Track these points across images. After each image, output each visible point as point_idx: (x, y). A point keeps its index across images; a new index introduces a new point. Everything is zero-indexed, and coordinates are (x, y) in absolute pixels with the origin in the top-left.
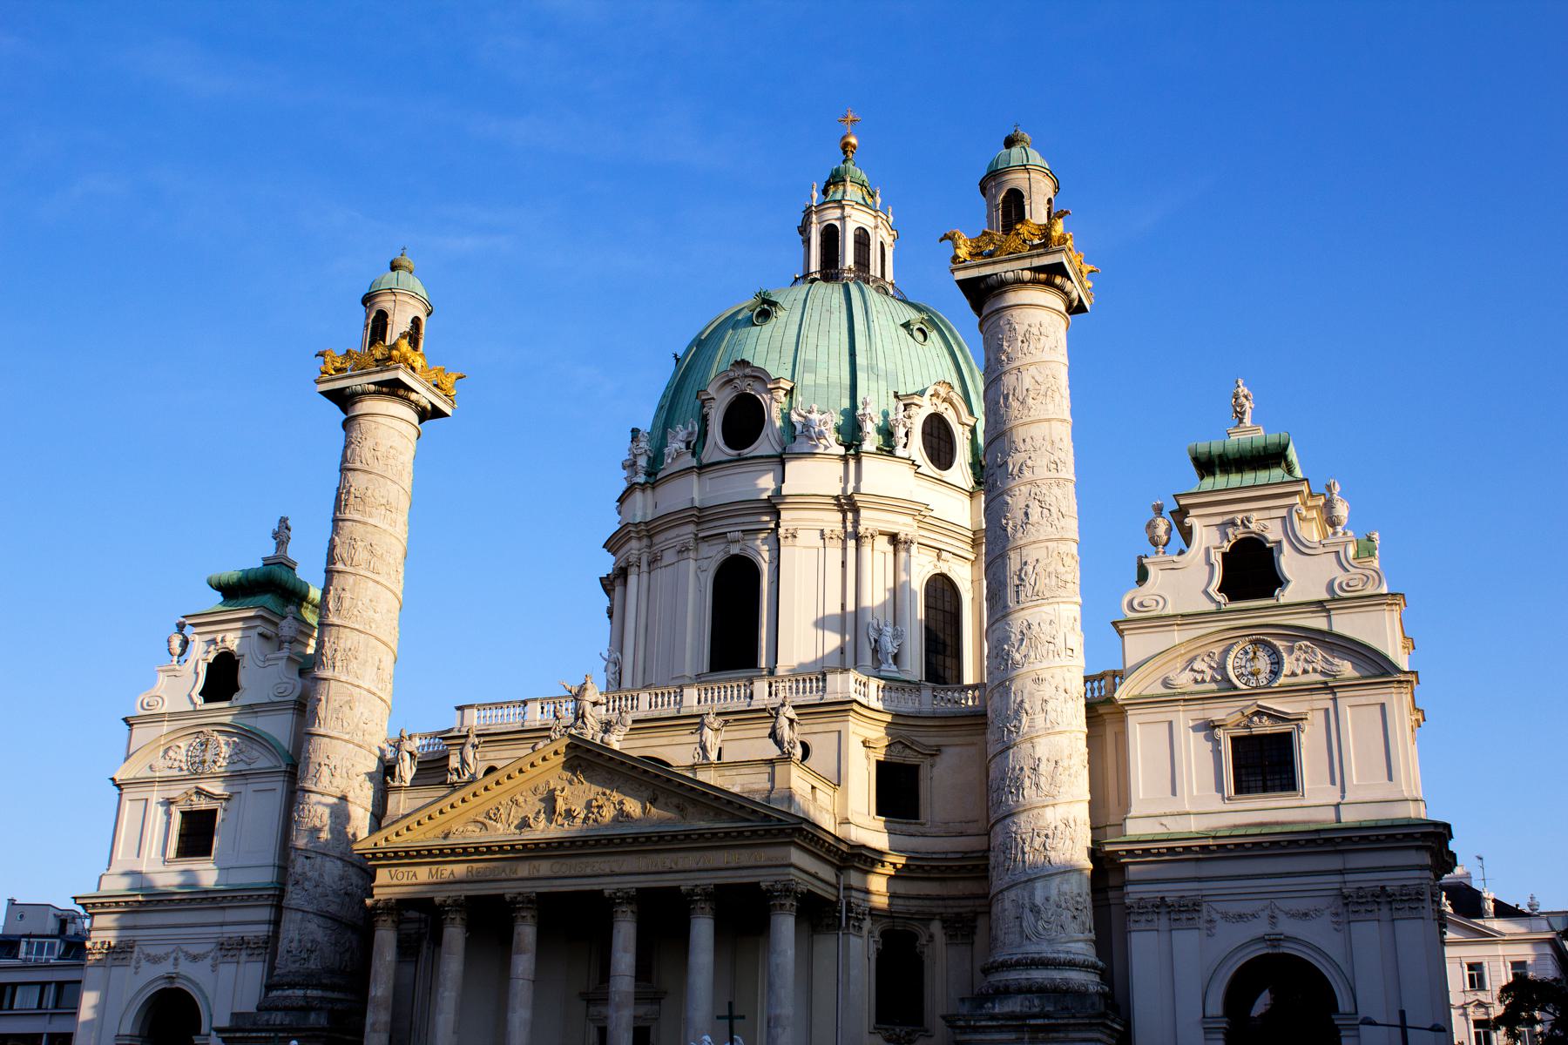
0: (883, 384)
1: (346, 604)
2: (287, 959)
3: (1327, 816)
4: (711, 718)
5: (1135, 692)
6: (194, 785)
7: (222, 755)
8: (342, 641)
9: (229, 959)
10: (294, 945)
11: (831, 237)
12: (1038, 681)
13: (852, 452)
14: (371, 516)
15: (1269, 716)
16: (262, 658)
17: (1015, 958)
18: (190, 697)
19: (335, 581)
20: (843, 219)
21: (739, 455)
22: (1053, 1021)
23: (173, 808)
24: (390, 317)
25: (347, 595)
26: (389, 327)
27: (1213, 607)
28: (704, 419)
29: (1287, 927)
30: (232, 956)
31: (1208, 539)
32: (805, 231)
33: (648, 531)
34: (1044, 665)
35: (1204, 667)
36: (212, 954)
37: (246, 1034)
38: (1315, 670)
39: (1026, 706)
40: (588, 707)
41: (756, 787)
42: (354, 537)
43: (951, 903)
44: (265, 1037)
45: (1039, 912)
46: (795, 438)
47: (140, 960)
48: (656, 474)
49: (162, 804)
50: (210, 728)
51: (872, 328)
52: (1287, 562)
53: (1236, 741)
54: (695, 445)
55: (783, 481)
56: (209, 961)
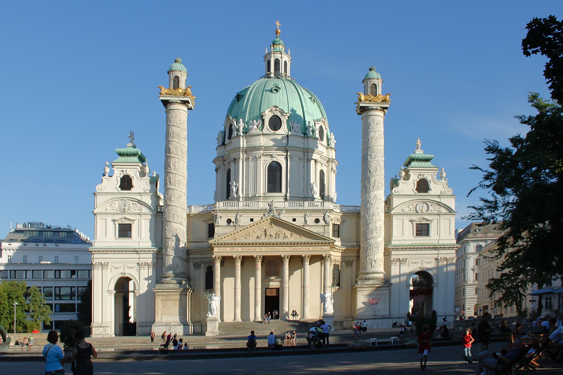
5: (395, 212)
6: (123, 216)
12: (377, 208)
13: (306, 135)
15: (425, 219)
21: (275, 133)
23: (116, 222)
28: (263, 121)
31: (414, 177)
34: (379, 205)
35: (412, 208)
38: (436, 210)
39: (375, 214)
40: (274, 209)
41: (320, 231)
43: (347, 258)
48: (246, 133)
50: (126, 199)
51: (305, 98)
53: (417, 224)
54: (260, 128)
55: (288, 142)
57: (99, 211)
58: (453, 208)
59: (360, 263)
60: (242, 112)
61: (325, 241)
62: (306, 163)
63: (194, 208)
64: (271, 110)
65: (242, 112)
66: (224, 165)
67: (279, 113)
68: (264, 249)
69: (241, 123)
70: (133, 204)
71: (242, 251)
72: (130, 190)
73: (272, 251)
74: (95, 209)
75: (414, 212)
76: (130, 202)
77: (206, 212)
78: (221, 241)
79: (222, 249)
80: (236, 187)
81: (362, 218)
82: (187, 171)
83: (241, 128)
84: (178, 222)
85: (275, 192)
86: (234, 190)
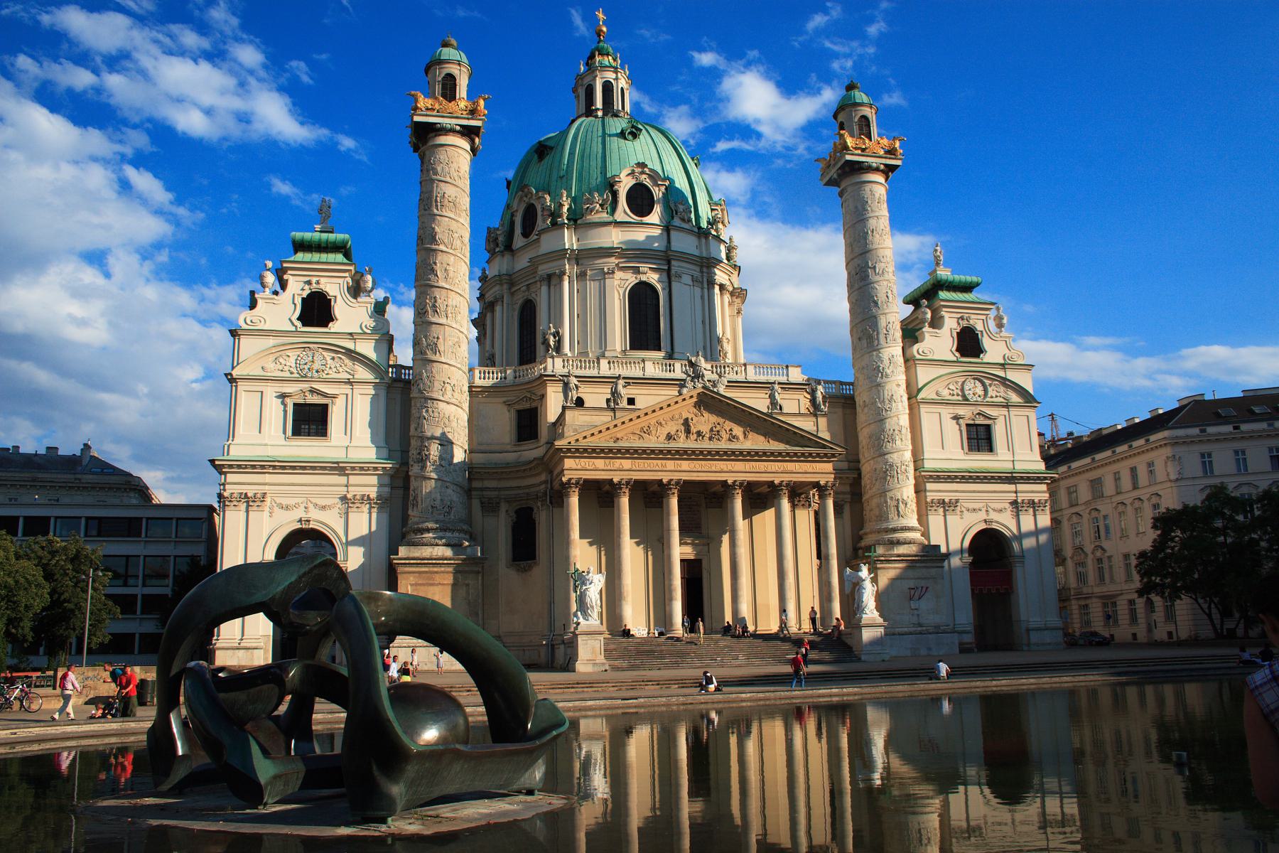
1: (451, 274)
2: (432, 513)
3: (1008, 466)
4: (776, 387)
7: (328, 366)
8: (450, 300)
9: (356, 510)
10: (438, 503)
11: (608, 88)
14: (460, 216)
15: (983, 415)
16: (354, 301)
18: (290, 319)
19: (439, 258)
20: (617, 79)
24: (458, 81)
25: (450, 268)
26: (458, 88)
27: (955, 359)
28: (615, 195)
29: (993, 516)
32: (582, 79)
37: (419, 561)
39: (894, 397)
42: (452, 228)
45: (906, 504)
46: (673, 218)
48: (575, 221)
49: (277, 397)
50: (316, 346)
52: (986, 342)
57: (245, 373)
58: (1031, 392)
61: (825, 451)
62: (706, 290)
63: (480, 373)
64: (632, 173)
65: (561, 178)
66: (512, 294)
67: (648, 180)
68: (685, 465)
69: (564, 199)
70: (333, 359)
71: (634, 468)
73: (703, 469)
74: (233, 368)
75: (960, 398)
76: (325, 354)
78: (583, 443)
79: (584, 463)
80: (555, 337)
84: (453, 401)
85: (647, 348)
86: (552, 343)
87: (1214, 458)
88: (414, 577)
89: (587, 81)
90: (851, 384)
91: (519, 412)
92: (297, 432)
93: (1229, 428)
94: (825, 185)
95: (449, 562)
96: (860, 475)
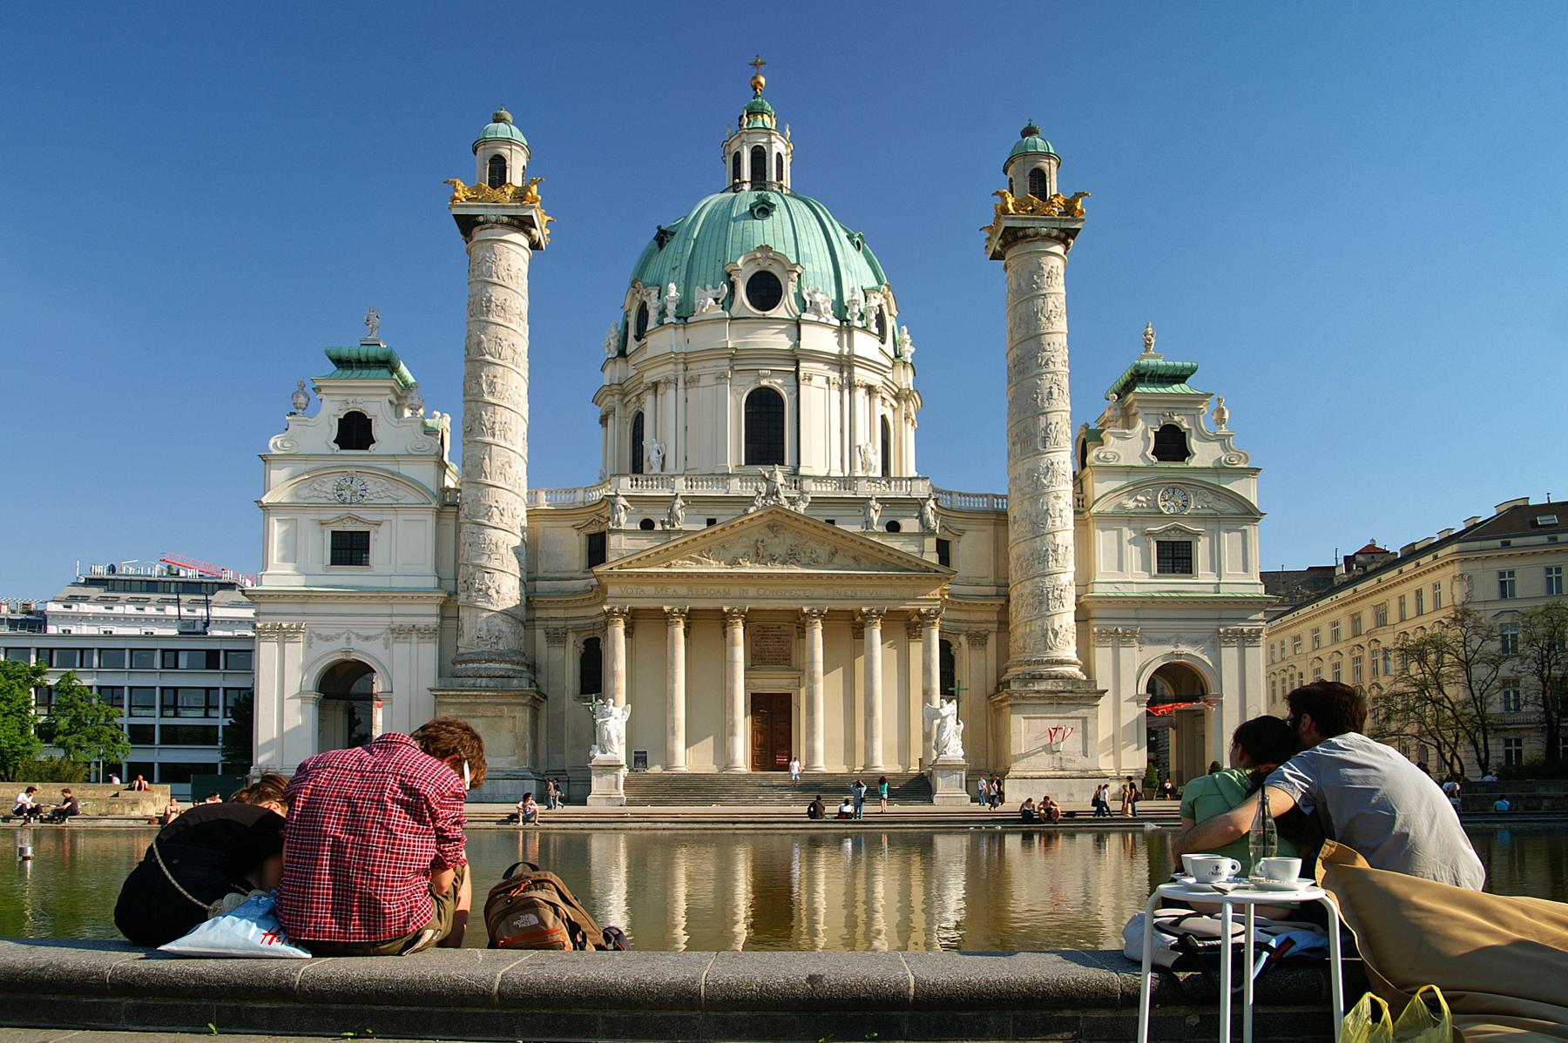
0: (854, 277)
2: (478, 643)
10: (484, 633)
11: (759, 156)
13: (845, 323)
17: (1045, 659)
20: (770, 143)
21: (764, 315)
22: (1074, 695)
28: (732, 286)
30: (404, 638)
33: (685, 359)
36: (384, 636)
37: (459, 693)
44: (476, 695)
45: (1057, 633)
47: (312, 637)
48: (686, 319)
54: (722, 303)
55: (799, 339)
56: (380, 642)
58: (1254, 501)
59: (1012, 639)
60: (676, 267)
65: (674, 269)
72: (367, 449)
77: (582, 505)
81: (1015, 523)
82: (529, 402)
83: (671, 308)
87: (1518, 579)
88: (455, 709)
89: (734, 148)
90: (1006, 497)
91: (591, 537)
92: (336, 561)
93: (1544, 539)
94: (991, 259)
95: (492, 694)
96: (1008, 601)
